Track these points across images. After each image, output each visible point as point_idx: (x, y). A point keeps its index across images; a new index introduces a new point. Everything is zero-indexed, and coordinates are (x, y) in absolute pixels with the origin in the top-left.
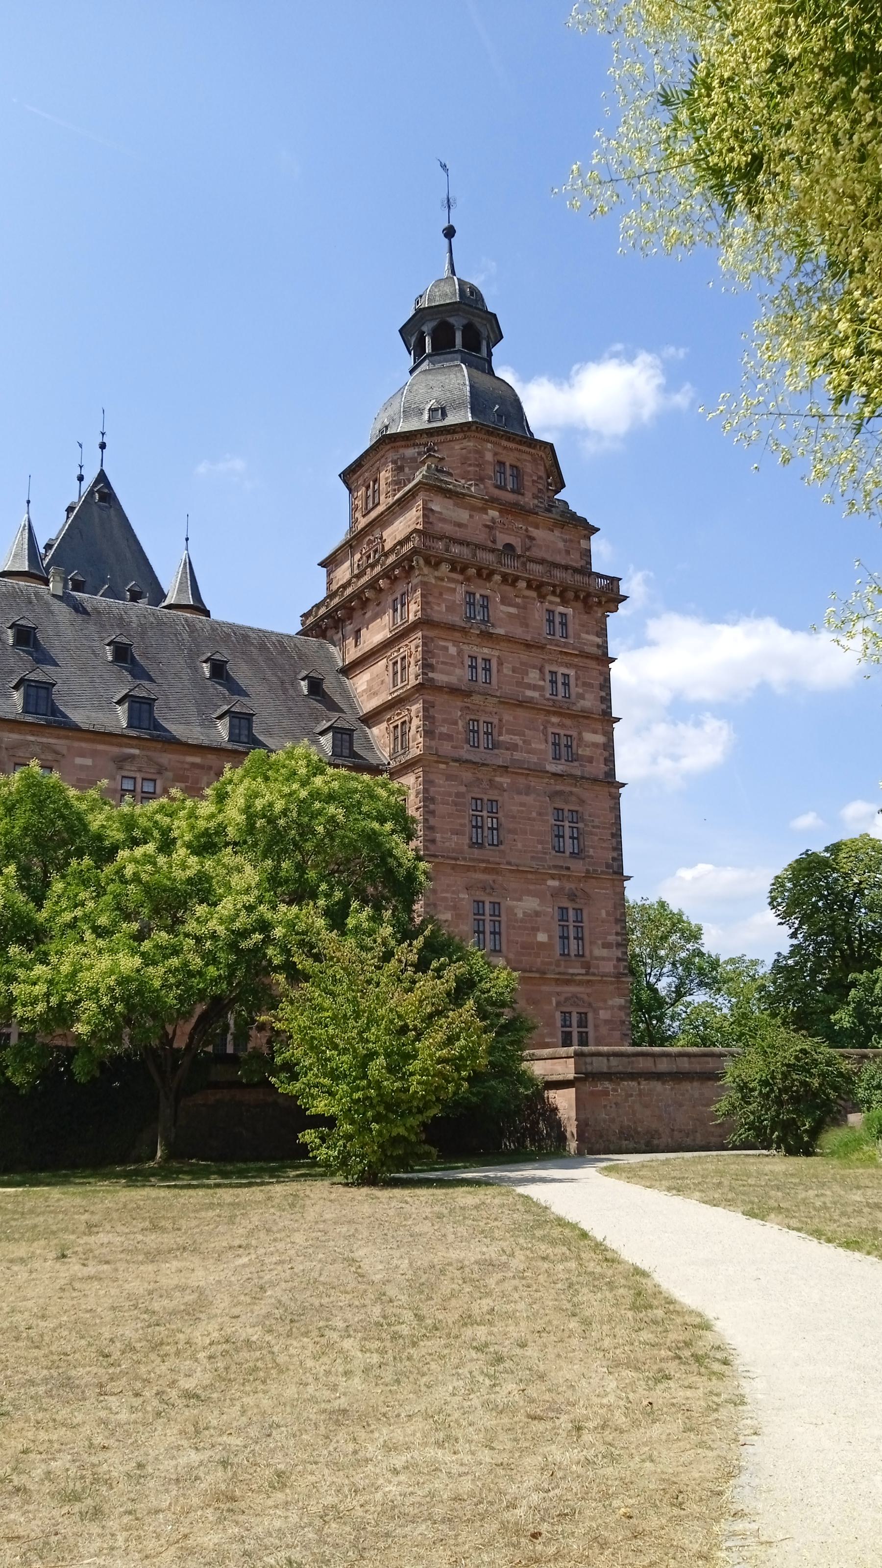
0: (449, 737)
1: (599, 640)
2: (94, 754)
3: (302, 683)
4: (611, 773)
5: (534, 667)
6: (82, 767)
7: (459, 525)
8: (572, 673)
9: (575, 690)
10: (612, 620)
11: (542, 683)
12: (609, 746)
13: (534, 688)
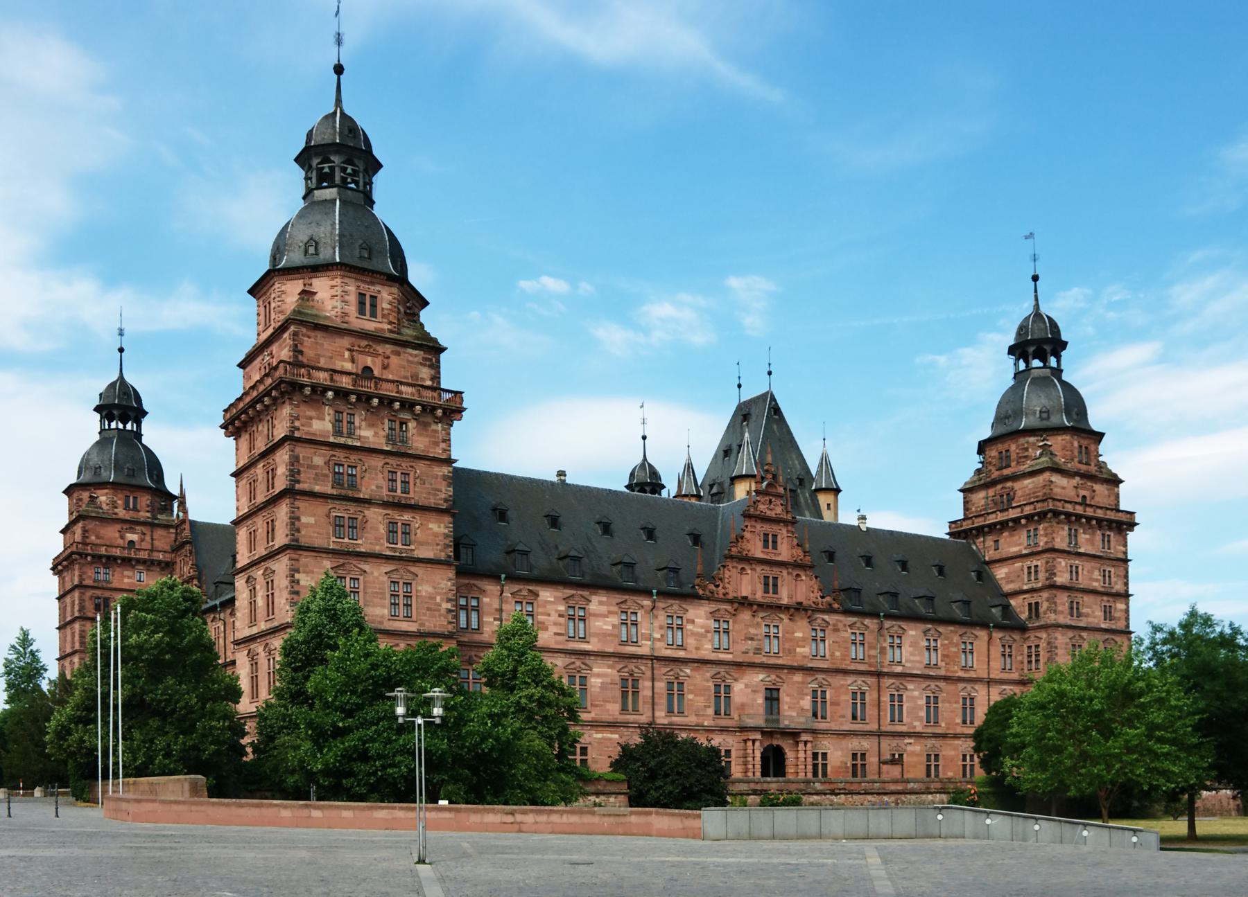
0: (1062, 612)
1: (1124, 549)
2: (915, 629)
3: (973, 574)
4: (1128, 626)
5: (1096, 568)
6: (912, 636)
7: (1064, 488)
8: (1113, 570)
9: (1113, 579)
10: (1131, 536)
11: (1099, 577)
12: (1127, 611)
13: (1097, 580)
